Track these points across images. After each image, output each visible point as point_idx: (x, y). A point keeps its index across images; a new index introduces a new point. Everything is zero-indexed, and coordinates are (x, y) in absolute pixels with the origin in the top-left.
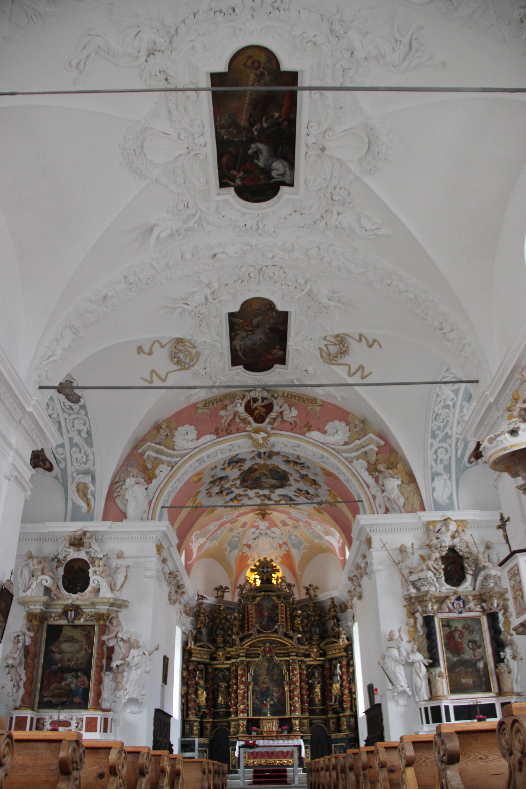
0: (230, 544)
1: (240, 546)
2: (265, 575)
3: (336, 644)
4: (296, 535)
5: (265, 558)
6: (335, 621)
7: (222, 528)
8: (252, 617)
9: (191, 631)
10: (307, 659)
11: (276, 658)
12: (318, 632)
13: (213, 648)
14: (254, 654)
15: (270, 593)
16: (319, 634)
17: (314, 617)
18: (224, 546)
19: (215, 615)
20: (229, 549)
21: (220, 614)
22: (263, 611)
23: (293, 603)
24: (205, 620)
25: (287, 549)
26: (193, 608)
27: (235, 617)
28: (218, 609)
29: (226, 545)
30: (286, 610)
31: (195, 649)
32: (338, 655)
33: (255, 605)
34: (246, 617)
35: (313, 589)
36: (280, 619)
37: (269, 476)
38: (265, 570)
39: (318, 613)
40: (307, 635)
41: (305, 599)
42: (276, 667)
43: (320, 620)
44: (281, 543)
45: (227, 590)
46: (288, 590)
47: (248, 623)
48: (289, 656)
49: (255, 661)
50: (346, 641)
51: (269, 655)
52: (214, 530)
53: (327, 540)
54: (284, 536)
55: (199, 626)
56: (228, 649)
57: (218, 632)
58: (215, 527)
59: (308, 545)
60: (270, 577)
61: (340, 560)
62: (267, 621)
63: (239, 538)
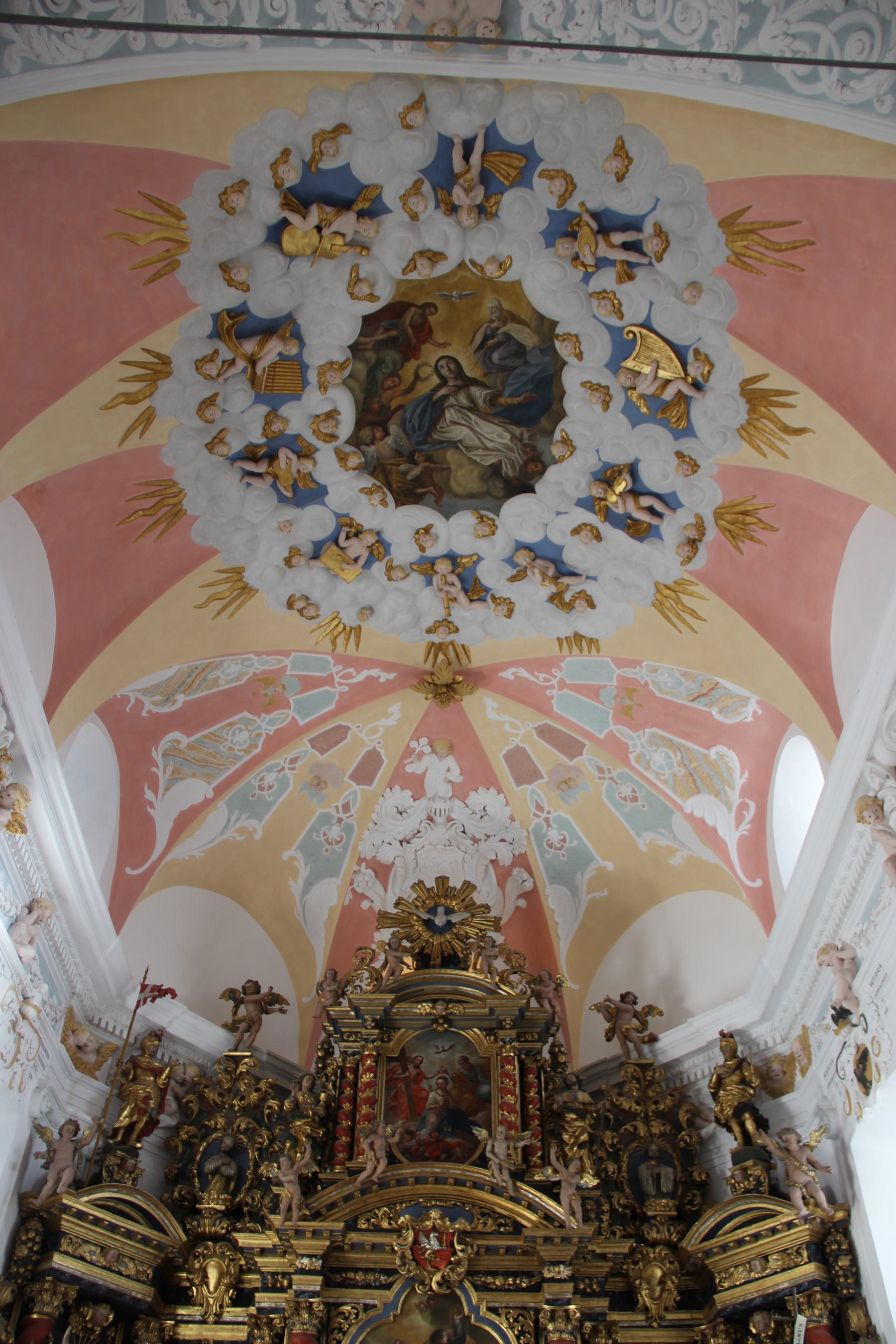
0: (309, 850)
1: (348, 864)
2: (436, 940)
3: (769, 1224)
4: (563, 824)
5: (442, 880)
6: (750, 1126)
7: (281, 759)
8: (371, 1102)
9: (74, 1126)
10: (615, 1316)
11: (474, 1296)
12: (667, 1186)
13: (176, 1232)
14: (366, 1271)
15: (456, 1009)
16: (671, 1195)
17: (647, 1120)
18: (285, 856)
19: (212, 1095)
20: (304, 872)
21: (233, 1092)
22: (424, 1084)
23: (556, 1064)
24: (161, 1108)
25: (529, 885)
26: (115, 1050)
27: (297, 1104)
28: (228, 1072)
29: (291, 853)
30: (524, 1088)
31: (81, 1215)
32: (783, 1281)
33: (390, 1059)
34: (347, 1106)
35: (636, 1015)
36: (497, 1114)
37: (478, 393)
38: (439, 921)
39: (662, 1107)
40: (619, 1200)
41: (604, 1062)
42: (468, 1338)
43: (671, 1137)
44: (506, 858)
45: (277, 1006)
46: (534, 1004)
47: (351, 1131)
48: (536, 1288)
49: (367, 1307)
50: (822, 1197)
51: (437, 1277)
52: (248, 758)
53: (691, 818)
54: (517, 823)
55: (124, 1120)
56: (243, 1239)
57: (210, 1166)
58: (254, 746)
59: (610, 866)
60: (457, 945)
61: (749, 889)
62: (438, 1129)
63: (349, 829)
